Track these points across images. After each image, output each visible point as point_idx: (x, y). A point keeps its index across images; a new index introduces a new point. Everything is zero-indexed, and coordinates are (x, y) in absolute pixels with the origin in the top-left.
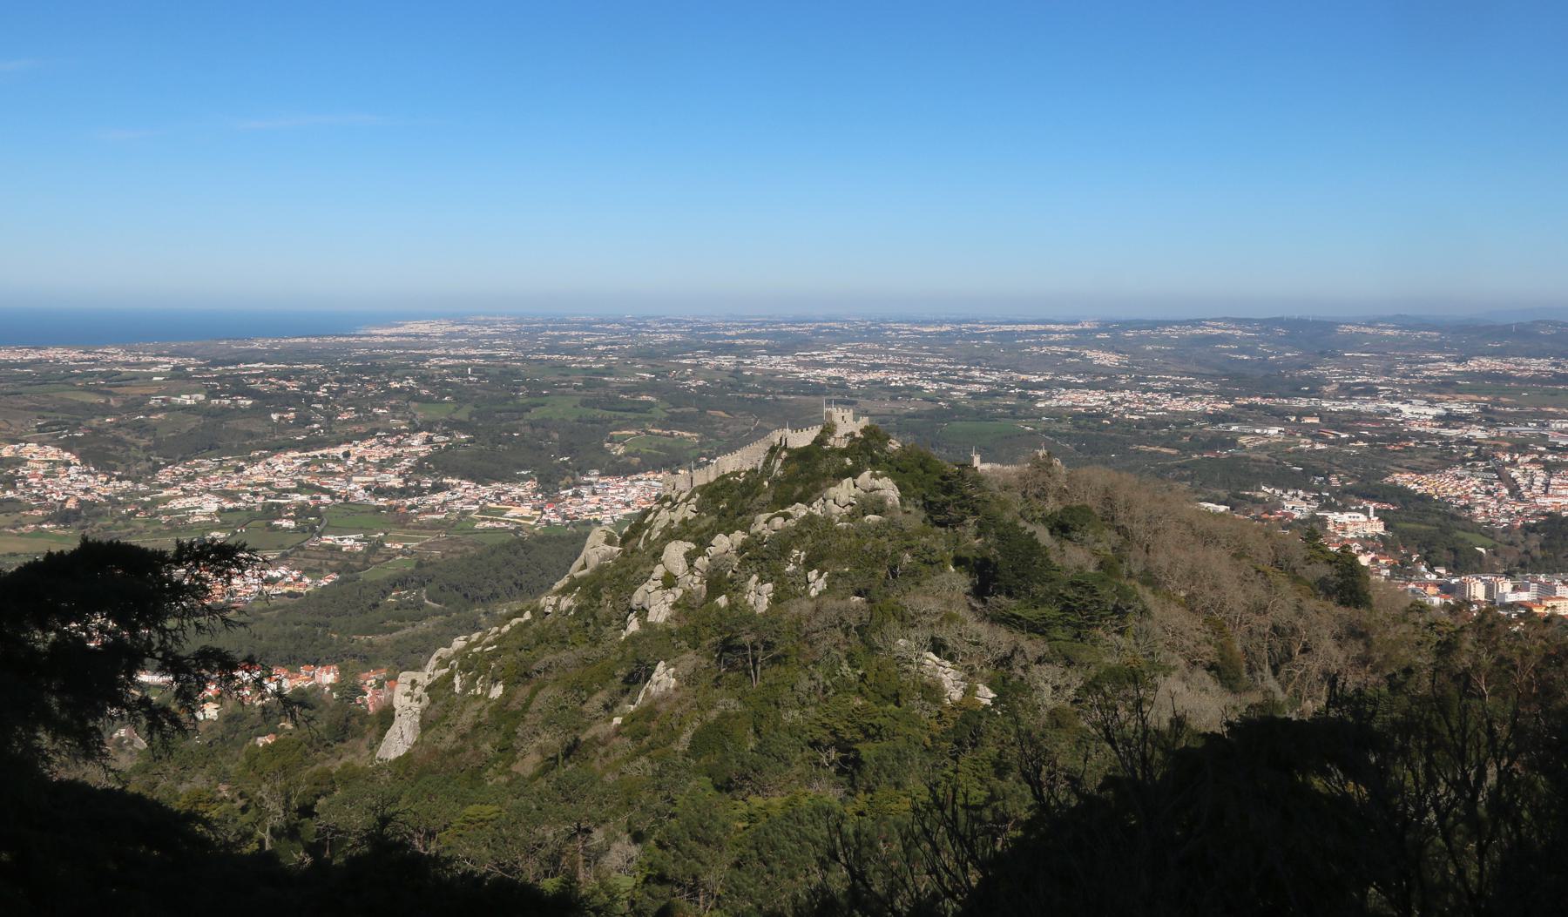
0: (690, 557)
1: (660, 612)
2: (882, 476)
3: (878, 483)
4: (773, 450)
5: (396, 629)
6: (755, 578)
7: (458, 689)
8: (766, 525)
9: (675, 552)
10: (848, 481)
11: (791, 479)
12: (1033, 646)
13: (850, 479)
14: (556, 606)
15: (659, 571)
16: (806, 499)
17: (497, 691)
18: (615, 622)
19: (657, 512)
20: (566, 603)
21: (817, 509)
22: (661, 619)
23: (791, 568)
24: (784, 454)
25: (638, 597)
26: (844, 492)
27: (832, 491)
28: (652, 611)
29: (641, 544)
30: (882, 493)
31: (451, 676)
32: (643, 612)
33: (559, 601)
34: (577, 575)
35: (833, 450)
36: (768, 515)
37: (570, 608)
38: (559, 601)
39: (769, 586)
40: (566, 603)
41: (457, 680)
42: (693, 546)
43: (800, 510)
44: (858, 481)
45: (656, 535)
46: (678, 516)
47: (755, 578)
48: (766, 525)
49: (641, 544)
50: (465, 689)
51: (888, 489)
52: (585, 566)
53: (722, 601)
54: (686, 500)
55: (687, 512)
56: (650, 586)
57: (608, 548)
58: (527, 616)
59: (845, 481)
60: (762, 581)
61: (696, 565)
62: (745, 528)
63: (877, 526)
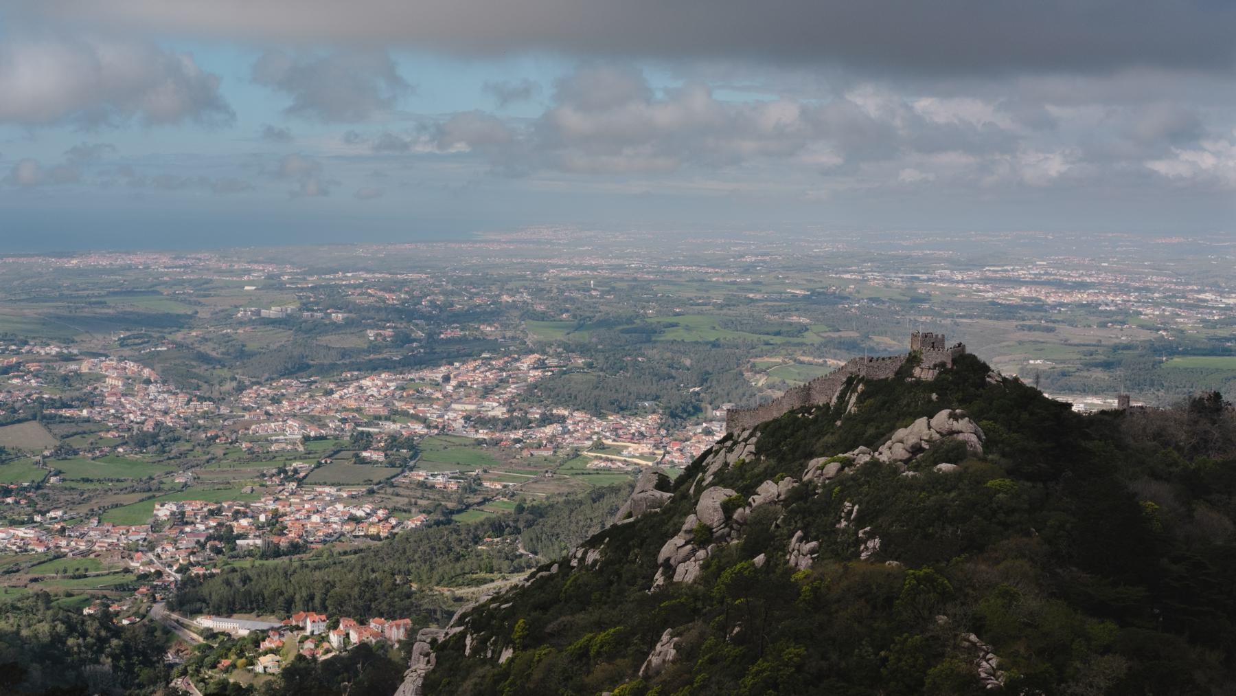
0: (728, 508)
1: (688, 572)
2: (962, 416)
3: (957, 426)
4: (850, 383)
5: (485, 581)
6: (799, 533)
7: (468, 652)
8: (822, 469)
9: (711, 502)
10: (921, 422)
11: (865, 418)
12: (1102, 629)
13: (924, 419)
14: (583, 559)
15: (690, 522)
16: (873, 443)
17: (507, 655)
18: (640, 582)
19: (717, 452)
20: (593, 556)
21: (884, 456)
22: (689, 578)
23: (844, 523)
24: (860, 387)
25: (666, 551)
26: (918, 430)
27: (901, 433)
28: (681, 569)
29: (691, 491)
30: (960, 437)
31: (463, 636)
32: (669, 569)
33: (585, 553)
34: (620, 523)
35: (919, 382)
36: (822, 460)
37: (595, 561)
38: (585, 553)
39: (814, 544)
40: (593, 556)
41: (468, 641)
42: (734, 494)
43: (862, 456)
44: (934, 422)
45: (709, 479)
46: (732, 459)
47: (799, 533)
48: (822, 469)
49: (691, 491)
50: (475, 651)
51: (967, 431)
52: (630, 515)
53: (760, 559)
54: (745, 440)
55: (743, 453)
56: (679, 540)
57: (658, 494)
58: (555, 569)
59: (918, 421)
60: (805, 539)
61: (735, 516)
62: (797, 475)
63: (946, 475)
